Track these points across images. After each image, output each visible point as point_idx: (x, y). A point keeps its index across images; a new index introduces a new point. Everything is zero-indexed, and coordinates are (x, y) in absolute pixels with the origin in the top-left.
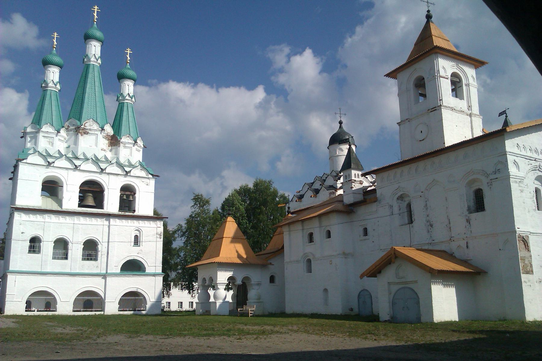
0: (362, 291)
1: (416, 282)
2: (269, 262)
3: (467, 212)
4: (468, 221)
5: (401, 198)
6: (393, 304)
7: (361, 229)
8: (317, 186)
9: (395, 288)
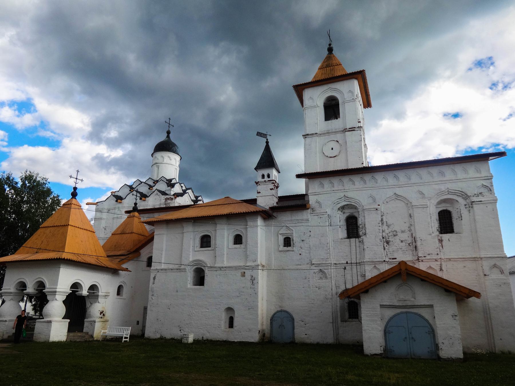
0: (278, 312)
1: (431, 306)
2: (124, 266)
3: (438, 233)
4: (441, 241)
5: (343, 208)
6: (386, 332)
7: (281, 239)
8: (144, 189)
9: (389, 313)
